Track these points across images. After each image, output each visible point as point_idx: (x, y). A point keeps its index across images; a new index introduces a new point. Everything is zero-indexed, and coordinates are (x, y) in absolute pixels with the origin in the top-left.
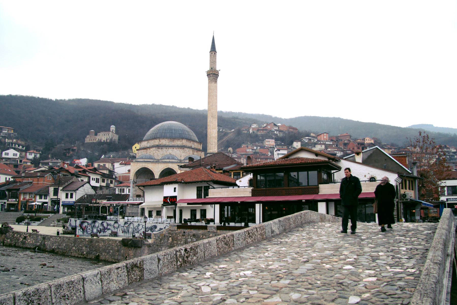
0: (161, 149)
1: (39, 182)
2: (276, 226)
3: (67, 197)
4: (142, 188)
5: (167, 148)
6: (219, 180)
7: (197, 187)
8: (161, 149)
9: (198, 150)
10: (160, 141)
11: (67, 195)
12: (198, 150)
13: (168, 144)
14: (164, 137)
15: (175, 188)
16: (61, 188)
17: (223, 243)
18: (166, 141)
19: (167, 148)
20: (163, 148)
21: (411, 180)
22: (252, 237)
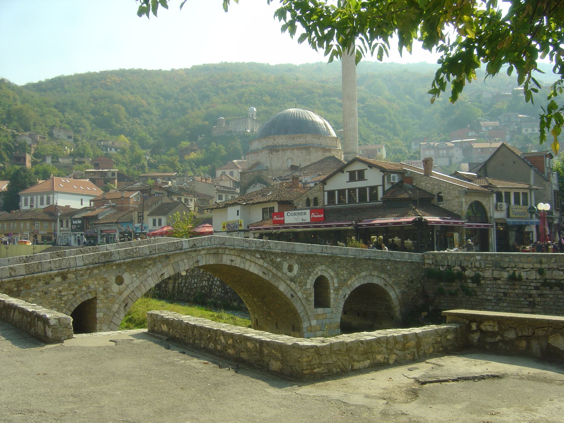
1: (124, 205)
3: (154, 224)
10: (274, 139)
11: (154, 221)
14: (278, 133)
15: (238, 211)
16: (146, 213)
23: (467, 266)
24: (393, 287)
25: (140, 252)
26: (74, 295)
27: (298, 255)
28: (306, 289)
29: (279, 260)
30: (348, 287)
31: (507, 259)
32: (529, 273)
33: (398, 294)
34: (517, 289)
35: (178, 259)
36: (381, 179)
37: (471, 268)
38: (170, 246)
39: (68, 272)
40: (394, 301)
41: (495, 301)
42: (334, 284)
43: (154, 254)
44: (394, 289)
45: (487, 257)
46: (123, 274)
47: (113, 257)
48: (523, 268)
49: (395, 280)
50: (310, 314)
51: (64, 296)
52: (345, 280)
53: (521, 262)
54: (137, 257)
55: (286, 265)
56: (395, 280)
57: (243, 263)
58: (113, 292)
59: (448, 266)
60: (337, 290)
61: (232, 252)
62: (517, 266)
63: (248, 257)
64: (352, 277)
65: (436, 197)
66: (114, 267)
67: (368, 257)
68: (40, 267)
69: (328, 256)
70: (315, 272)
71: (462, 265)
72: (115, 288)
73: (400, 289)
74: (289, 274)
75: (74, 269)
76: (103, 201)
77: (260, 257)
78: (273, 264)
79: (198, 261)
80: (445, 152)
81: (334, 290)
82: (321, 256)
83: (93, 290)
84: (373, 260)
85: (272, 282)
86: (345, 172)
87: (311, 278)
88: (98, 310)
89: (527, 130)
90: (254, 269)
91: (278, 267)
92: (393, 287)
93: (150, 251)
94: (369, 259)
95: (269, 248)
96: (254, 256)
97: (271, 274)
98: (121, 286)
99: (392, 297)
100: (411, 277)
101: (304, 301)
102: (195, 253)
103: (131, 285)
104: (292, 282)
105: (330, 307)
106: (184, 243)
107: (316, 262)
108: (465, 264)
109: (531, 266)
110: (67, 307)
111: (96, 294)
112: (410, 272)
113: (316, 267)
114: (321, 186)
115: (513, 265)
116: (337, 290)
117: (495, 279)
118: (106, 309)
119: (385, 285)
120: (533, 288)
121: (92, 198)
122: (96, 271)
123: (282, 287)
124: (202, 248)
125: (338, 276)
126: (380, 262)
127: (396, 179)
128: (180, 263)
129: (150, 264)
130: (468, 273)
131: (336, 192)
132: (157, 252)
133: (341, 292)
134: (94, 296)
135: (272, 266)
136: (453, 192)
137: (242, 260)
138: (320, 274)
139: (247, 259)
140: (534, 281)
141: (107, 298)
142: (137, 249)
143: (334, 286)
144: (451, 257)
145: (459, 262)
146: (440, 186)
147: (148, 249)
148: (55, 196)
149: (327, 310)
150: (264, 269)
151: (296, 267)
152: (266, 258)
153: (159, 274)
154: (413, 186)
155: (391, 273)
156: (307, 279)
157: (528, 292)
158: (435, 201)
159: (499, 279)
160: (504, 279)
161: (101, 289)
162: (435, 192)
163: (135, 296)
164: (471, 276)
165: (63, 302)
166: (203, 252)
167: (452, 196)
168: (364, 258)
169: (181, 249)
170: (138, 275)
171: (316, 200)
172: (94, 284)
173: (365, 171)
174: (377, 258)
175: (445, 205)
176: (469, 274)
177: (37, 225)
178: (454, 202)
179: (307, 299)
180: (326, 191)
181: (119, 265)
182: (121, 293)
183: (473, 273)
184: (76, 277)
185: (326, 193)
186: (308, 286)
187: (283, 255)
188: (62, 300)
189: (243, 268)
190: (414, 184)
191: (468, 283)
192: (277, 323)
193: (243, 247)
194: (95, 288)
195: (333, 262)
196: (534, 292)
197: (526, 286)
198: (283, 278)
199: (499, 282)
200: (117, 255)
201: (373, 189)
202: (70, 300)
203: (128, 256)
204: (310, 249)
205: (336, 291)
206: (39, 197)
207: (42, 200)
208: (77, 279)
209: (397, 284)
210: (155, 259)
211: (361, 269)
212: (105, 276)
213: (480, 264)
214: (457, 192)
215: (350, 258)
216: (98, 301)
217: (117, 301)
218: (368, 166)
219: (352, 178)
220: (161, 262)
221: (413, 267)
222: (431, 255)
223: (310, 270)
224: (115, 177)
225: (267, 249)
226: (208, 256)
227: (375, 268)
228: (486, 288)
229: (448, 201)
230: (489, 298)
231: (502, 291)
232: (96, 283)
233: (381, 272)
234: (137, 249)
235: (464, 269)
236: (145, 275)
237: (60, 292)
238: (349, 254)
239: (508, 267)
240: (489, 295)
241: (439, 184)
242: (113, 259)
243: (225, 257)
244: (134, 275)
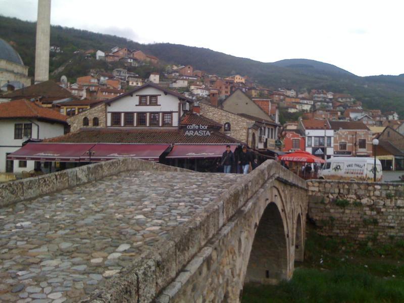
2: (84, 173)
6: (44, 116)
7: (16, 125)
9: (22, 75)
12: (22, 75)
17: (7, 191)
21: (271, 127)
22: (49, 186)
36: (177, 105)
41: (399, 228)
71: (358, 193)
80: (76, 92)
86: (134, 95)
89: (132, 83)
114: (104, 107)
130: (365, 201)
136: (241, 123)
145: (353, 191)
146: (229, 117)
158: (222, 131)
162: (223, 122)
164: (368, 204)
167: (241, 126)
175: (232, 134)
176: (366, 202)
185: (109, 116)
213: (381, 193)
214: (245, 124)
219: (141, 104)
229: (236, 131)
230: (391, 225)
235: (359, 197)
240: (391, 223)
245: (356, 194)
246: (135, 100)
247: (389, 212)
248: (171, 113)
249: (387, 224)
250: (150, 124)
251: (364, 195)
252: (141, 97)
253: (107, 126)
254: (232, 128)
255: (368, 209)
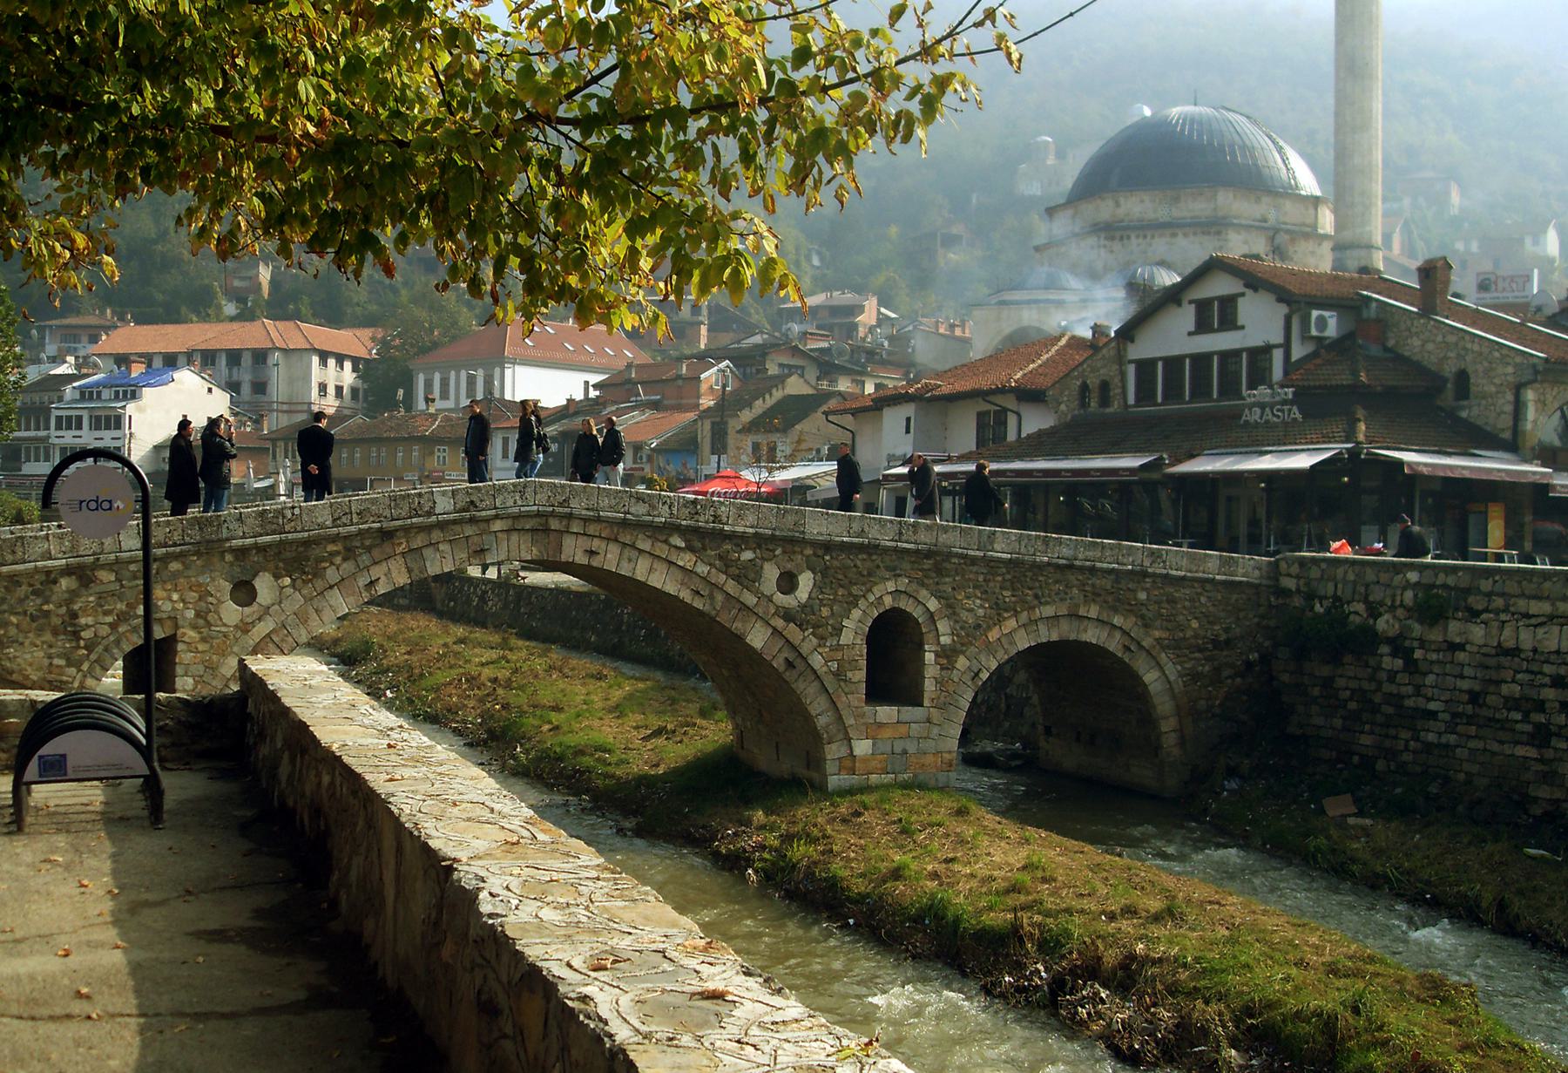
0: (1122, 238)
4: (848, 420)
5: (1145, 237)
8: (1122, 238)
10: (1118, 205)
13: (1151, 215)
16: (734, 425)
18: (1142, 201)
19: (1145, 237)
20: (1129, 238)
23: (1382, 604)
24: (1154, 658)
25: (304, 516)
26: (113, 626)
27: (814, 544)
28: (839, 647)
29: (748, 555)
30: (990, 649)
31: (1486, 585)
32: (1540, 631)
33: (1172, 678)
34: (1506, 682)
35: (418, 541)
36: (1281, 323)
37: (1393, 608)
38: (397, 505)
39: (96, 565)
40: (1156, 700)
42: (938, 636)
43: (345, 525)
44: (1158, 663)
45: (1436, 576)
46: (255, 575)
47: (225, 531)
48: (1527, 616)
49: (1164, 635)
50: (850, 721)
51: (88, 626)
52: (978, 626)
53: (1523, 595)
54: (296, 531)
55: (771, 573)
56: (1164, 635)
57: (630, 560)
58: (225, 625)
59: (1336, 598)
60: (947, 656)
61: (592, 529)
62: (1512, 609)
63: (644, 545)
64: (1005, 619)
65: (1449, 385)
66: (229, 557)
67: (1064, 562)
68: (19, 550)
69: (917, 551)
70: (872, 598)
71: (1371, 598)
72: (231, 613)
73: (1180, 663)
74: (780, 598)
75: (112, 556)
76: (627, 387)
77: (683, 545)
78: (727, 566)
79: (482, 550)
81: (937, 655)
82: (895, 549)
83: (164, 615)
84: (1081, 569)
85: (723, 619)
87: (856, 614)
88: (179, 670)
90: (661, 579)
91: (747, 576)
92: (1154, 658)
93: (336, 516)
94: (1071, 567)
95: (716, 518)
96: (666, 542)
97: (719, 597)
98: (247, 610)
99: (1150, 688)
100: (1227, 630)
101: (829, 682)
102: (474, 528)
103: (277, 607)
104: (792, 625)
105: (918, 703)
106: (438, 499)
107: (878, 567)
108: (1377, 595)
109: (1546, 608)
110: (93, 657)
111: (177, 627)
112: (1222, 614)
113: (876, 584)
115: (1499, 602)
116: (947, 656)
117: (1454, 647)
118: (201, 668)
119: (1127, 648)
120: (1547, 680)
121: (595, 378)
122: (175, 566)
123: (757, 638)
124: (493, 512)
125: (954, 613)
126: (1113, 577)
127: (1332, 325)
128: (428, 552)
129: (333, 554)
131: (1160, 364)
132: (355, 521)
133: (962, 662)
134: (169, 632)
135: (725, 573)
136: (1500, 370)
137: (627, 552)
138: (888, 602)
139: (641, 551)
140: (1553, 658)
141: (204, 640)
142: (297, 511)
143: (939, 643)
144: (1346, 572)
145: (1362, 590)
146: (1465, 349)
147: (327, 512)
148: (508, 372)
149: (909, 712)
150: (697, 580)
151: (806, 581)
152: (704, 548)
153: (363, 581)
154: (1386, 349)
155: (1150, 615)
156: (842, 617)
157: (1533, 694)
158: (1448, 398)
159: (1461, 647)
160: (1475, 649)
161: (191, 614)
162: (1449, 369)
163: (290, 639)
164: (1391, 634)
165: (82, 643)
166: (497, 526)
167: (1497, 381)
168: (1049, 564)
169: (429, 514)
170: (299, 582)
171: (1105, 386)
172: (170, 599)
173: (1240, 301)
174: (1098, 565)
175: (1475, 411)
176: (1385, 626)
177: (442, 455)
178: (1502, 401)
179: (838, 675)
180: (1131, 362)
181: (241, 552)
182: (245, 627)
183: (1397, 626)
184: (119, 580)
185: (1131, 370)
186: (846, 637)
187: (760, 542)
188: (79, 638)
189: (629, 574)
190: (1391, 343)
191: (1382, 656)
192: (777, 747)
193: (625, 513)
194: (174, 609)
195: (939, 571)
196: (1549, 694)
197: (1532, 672)
198: (760, 611)
199: (1461, 656)
200: (234, 525)
201: (1260, 354)
202: (103, 638)
203: (269, 527)
204: (856, 527)
205: (947, 657)
206: (463, 374)
207: (471, 381)
208: (122, 586)
209: (1168, 647)
210: (348, 537)
211: (1036, 596)
212: (201, 580)
215: (1000, 560)
216: (180, 647)
217: (235, 649)
218: (1247, 286)
219: (1203, 326)
220: (369, 549)
221: (1235, 597)
222: (1296, 565)
223: (855, 590)
224: (701, 318)
225: (707, 522)
226: (515, 537)
227: (1094, 596)
228: (1425, 674)
229: (1484, 398)
230: (1433, 706)
231: (1465, 685)
232: (175, 597)
233: (1115, 610)
234: (297, 511)
236: (319, 584)
237: (74, 615)
238: (997, 546)
239: (1486, 610)
241: (1461, 344)
242: (225, 534)
243: (568, 542)
244: (287, 581)
245: (1366, 601)
246: (1185, 317)
247: (1432, 662)
248: (1267, 349)
249: (1421, 702)
250: (1221, 393)
251: (1382, 604)
252: (1203, 307)
253: (1126, 406)
254: (1473, 389)
255: (1385, 649)
